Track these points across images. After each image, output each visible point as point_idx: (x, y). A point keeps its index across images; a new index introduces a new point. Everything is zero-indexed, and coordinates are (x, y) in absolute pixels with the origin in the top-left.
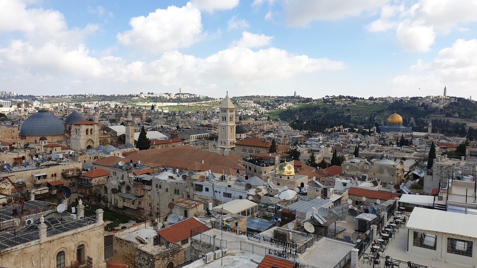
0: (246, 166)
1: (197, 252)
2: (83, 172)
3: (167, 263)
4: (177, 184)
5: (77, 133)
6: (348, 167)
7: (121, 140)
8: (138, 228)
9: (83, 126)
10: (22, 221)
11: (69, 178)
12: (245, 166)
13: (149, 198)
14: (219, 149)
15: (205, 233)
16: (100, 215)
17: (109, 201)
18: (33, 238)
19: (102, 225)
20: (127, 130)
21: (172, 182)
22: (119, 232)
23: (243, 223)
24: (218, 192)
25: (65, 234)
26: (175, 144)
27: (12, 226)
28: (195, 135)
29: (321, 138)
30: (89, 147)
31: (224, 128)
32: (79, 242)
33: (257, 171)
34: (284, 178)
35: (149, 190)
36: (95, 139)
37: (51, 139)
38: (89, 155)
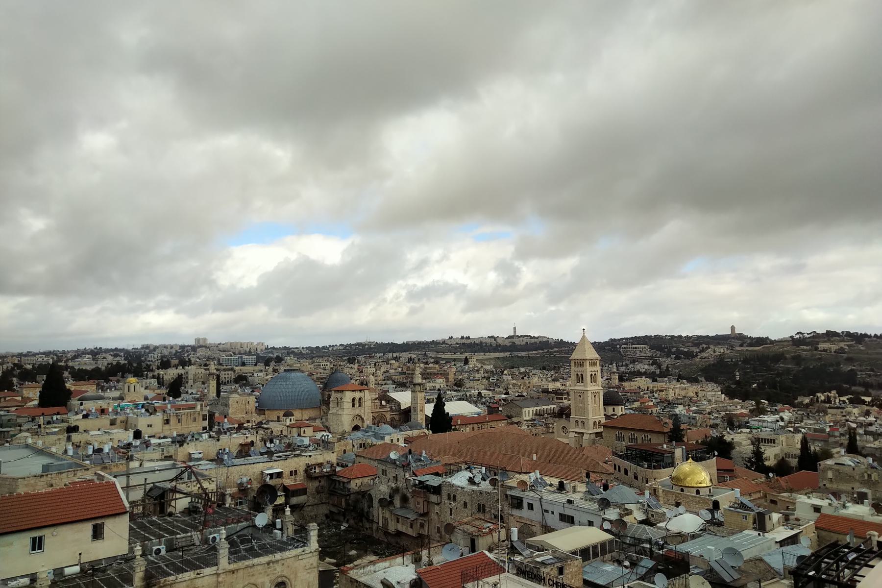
0: (619, 467)
2: (338, 469)
4: (481, 493)
5: (338, 406)
6: (830, 474)
7: (405, 416)
8: (390, 565)
9: (347, 392)
10: (204, 537)
11: (316, 478)
12: (617, 467)
13: (436, 517)
14: (572, 435)
16: (312, 533)
17: (376, 520)
18: (211, 564)
19: (315, 551)
20: (414, 399)
21: (473, 491)
22: (358, 569)
23: (575, 569)
24: (550, 512)
25: (256, 561)
28: (531, 409)
29: (787, 415)
30: (356, 428)
31: (582, 394)
32: (278, 577)
33: (640, 478)
34: (688, 492)
35: (436, 504)
36: (366, 414)
37: (300, 415)
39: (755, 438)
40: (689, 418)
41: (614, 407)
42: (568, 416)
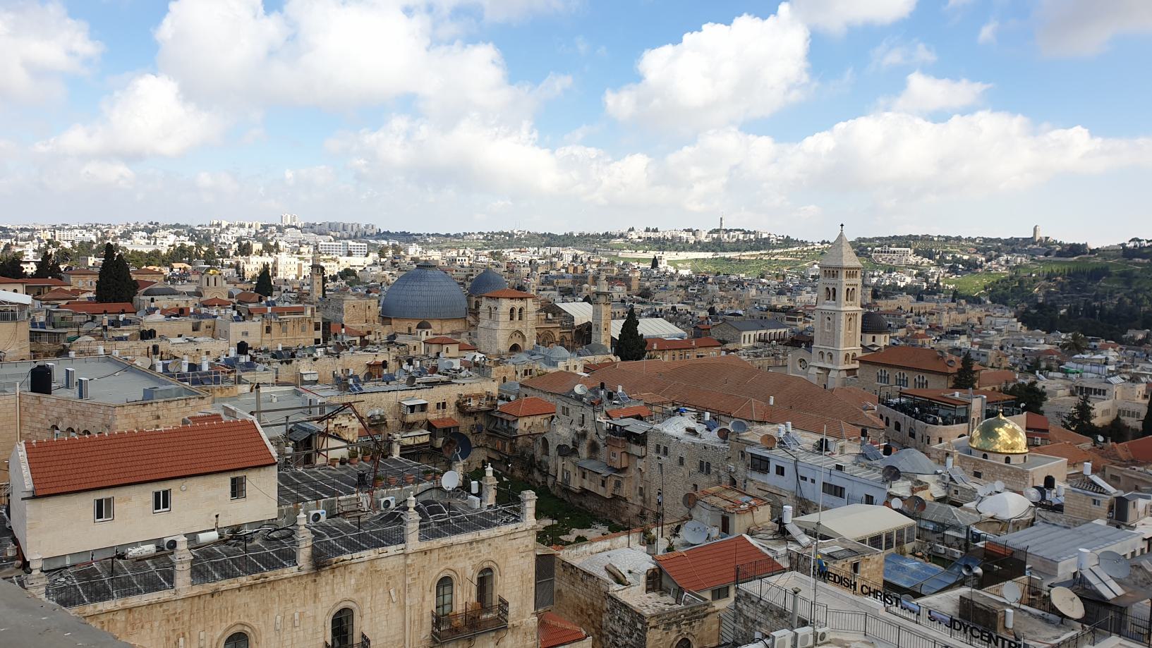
0: (887, 418)
1: (750, 624)
2: (500, 403)
3: (675, 640)
7: (583, 336)
10: (374, 500)
11: (471, 414)
12: (884, 419)
13: (638, 475)
14: (814, 371)
15: (773, 579)
17: (552, 472)
20: (596, 314)
21: (694, 444)
23: (874, 566)
24: (809, 480)
25: (455, 539)
26: (702, 352)
27: (354, 508)
28: (752, 333)
31: (831, 317)
33: (918, 435)
34: (994, 459)
35: (639, 457)
37: (440, 327)
38: (513, 366)
39: (1077, 387)
40: (978, 354)
41: (876, 336)
42: (809, 343)
